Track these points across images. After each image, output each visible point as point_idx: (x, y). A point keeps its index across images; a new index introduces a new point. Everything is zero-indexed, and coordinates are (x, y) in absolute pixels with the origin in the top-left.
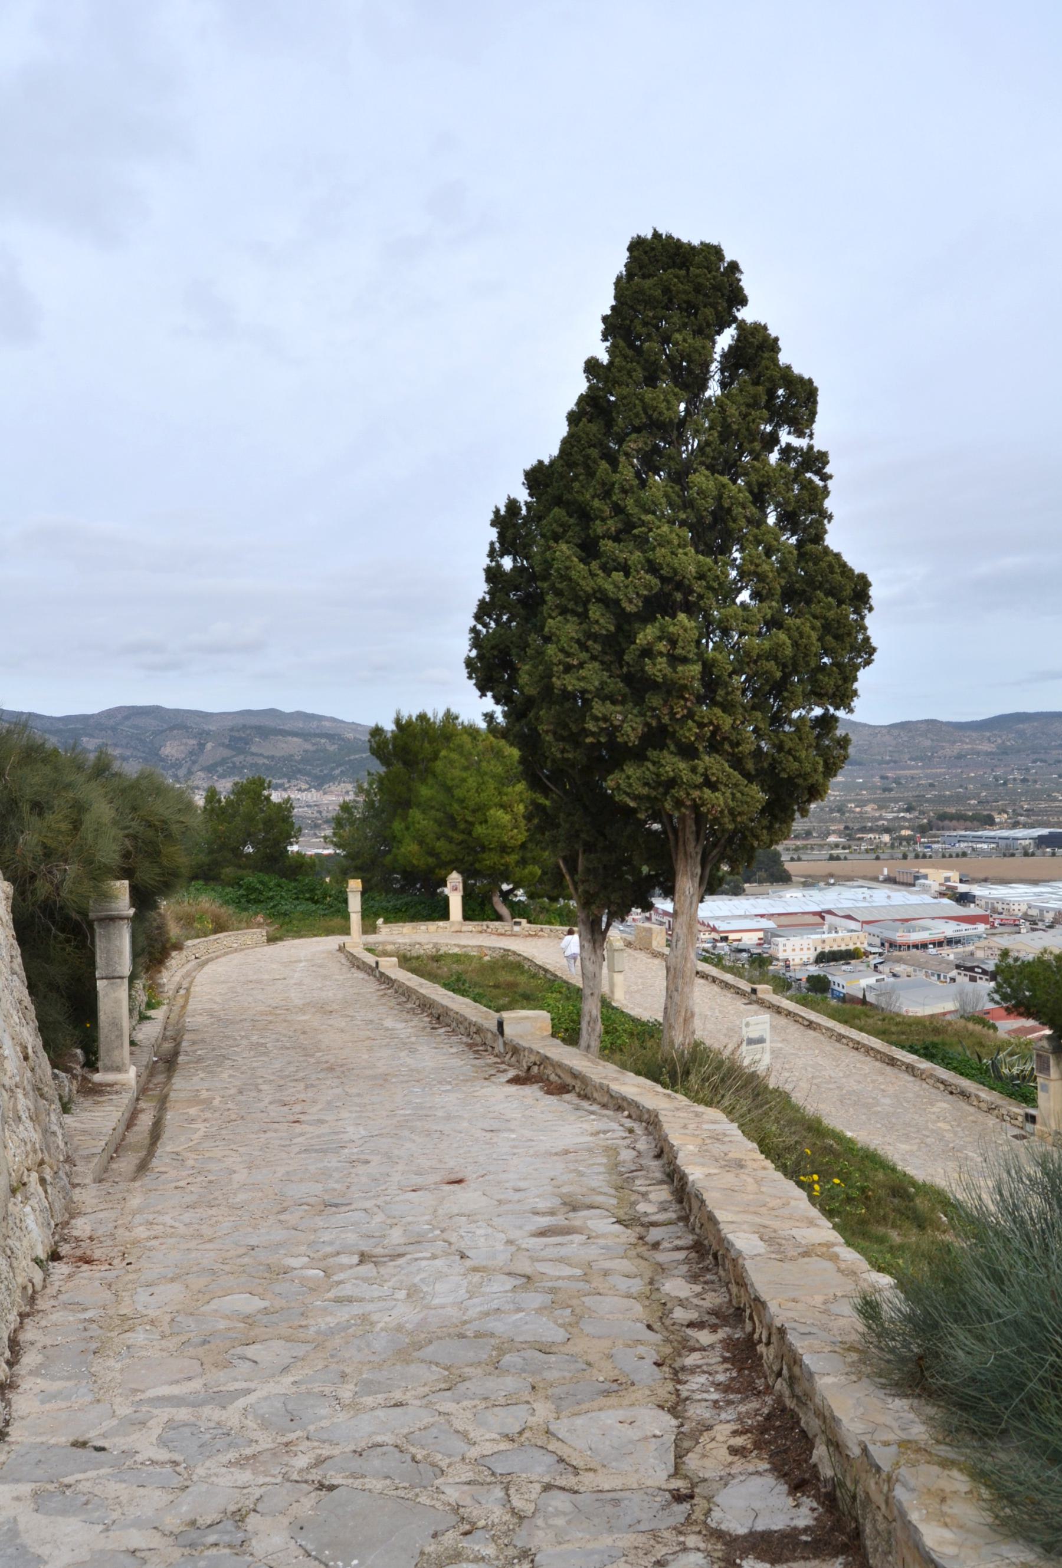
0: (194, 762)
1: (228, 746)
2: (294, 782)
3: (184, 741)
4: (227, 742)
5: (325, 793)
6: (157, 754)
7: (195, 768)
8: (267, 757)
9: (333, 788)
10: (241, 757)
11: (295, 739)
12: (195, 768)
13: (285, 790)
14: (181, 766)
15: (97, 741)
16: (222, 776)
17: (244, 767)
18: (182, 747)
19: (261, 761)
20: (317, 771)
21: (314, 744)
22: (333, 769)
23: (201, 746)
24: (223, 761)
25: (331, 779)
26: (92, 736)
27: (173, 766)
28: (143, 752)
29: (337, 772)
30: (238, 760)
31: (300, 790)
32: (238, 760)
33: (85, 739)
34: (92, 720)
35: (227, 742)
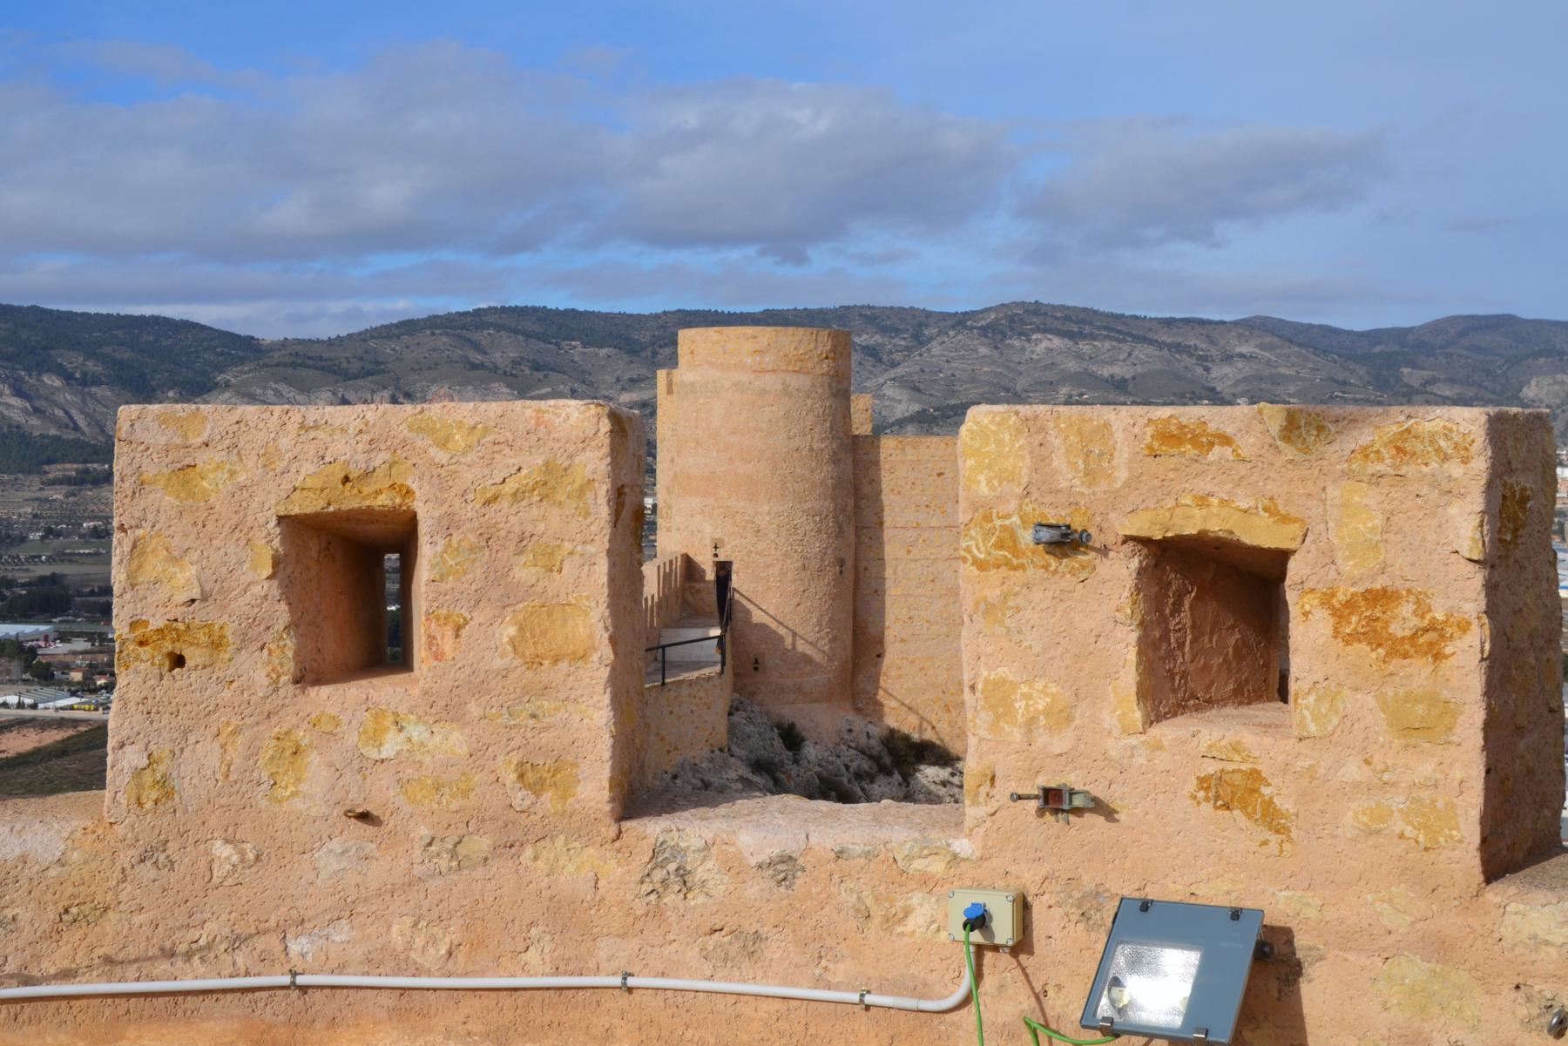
3: (1559, 377)
15: (1424, 373)
18: (1556, 387)
26: (1415, 366)
28: (1494, 392)
33: (1405, 371)
34: (1411, 337)
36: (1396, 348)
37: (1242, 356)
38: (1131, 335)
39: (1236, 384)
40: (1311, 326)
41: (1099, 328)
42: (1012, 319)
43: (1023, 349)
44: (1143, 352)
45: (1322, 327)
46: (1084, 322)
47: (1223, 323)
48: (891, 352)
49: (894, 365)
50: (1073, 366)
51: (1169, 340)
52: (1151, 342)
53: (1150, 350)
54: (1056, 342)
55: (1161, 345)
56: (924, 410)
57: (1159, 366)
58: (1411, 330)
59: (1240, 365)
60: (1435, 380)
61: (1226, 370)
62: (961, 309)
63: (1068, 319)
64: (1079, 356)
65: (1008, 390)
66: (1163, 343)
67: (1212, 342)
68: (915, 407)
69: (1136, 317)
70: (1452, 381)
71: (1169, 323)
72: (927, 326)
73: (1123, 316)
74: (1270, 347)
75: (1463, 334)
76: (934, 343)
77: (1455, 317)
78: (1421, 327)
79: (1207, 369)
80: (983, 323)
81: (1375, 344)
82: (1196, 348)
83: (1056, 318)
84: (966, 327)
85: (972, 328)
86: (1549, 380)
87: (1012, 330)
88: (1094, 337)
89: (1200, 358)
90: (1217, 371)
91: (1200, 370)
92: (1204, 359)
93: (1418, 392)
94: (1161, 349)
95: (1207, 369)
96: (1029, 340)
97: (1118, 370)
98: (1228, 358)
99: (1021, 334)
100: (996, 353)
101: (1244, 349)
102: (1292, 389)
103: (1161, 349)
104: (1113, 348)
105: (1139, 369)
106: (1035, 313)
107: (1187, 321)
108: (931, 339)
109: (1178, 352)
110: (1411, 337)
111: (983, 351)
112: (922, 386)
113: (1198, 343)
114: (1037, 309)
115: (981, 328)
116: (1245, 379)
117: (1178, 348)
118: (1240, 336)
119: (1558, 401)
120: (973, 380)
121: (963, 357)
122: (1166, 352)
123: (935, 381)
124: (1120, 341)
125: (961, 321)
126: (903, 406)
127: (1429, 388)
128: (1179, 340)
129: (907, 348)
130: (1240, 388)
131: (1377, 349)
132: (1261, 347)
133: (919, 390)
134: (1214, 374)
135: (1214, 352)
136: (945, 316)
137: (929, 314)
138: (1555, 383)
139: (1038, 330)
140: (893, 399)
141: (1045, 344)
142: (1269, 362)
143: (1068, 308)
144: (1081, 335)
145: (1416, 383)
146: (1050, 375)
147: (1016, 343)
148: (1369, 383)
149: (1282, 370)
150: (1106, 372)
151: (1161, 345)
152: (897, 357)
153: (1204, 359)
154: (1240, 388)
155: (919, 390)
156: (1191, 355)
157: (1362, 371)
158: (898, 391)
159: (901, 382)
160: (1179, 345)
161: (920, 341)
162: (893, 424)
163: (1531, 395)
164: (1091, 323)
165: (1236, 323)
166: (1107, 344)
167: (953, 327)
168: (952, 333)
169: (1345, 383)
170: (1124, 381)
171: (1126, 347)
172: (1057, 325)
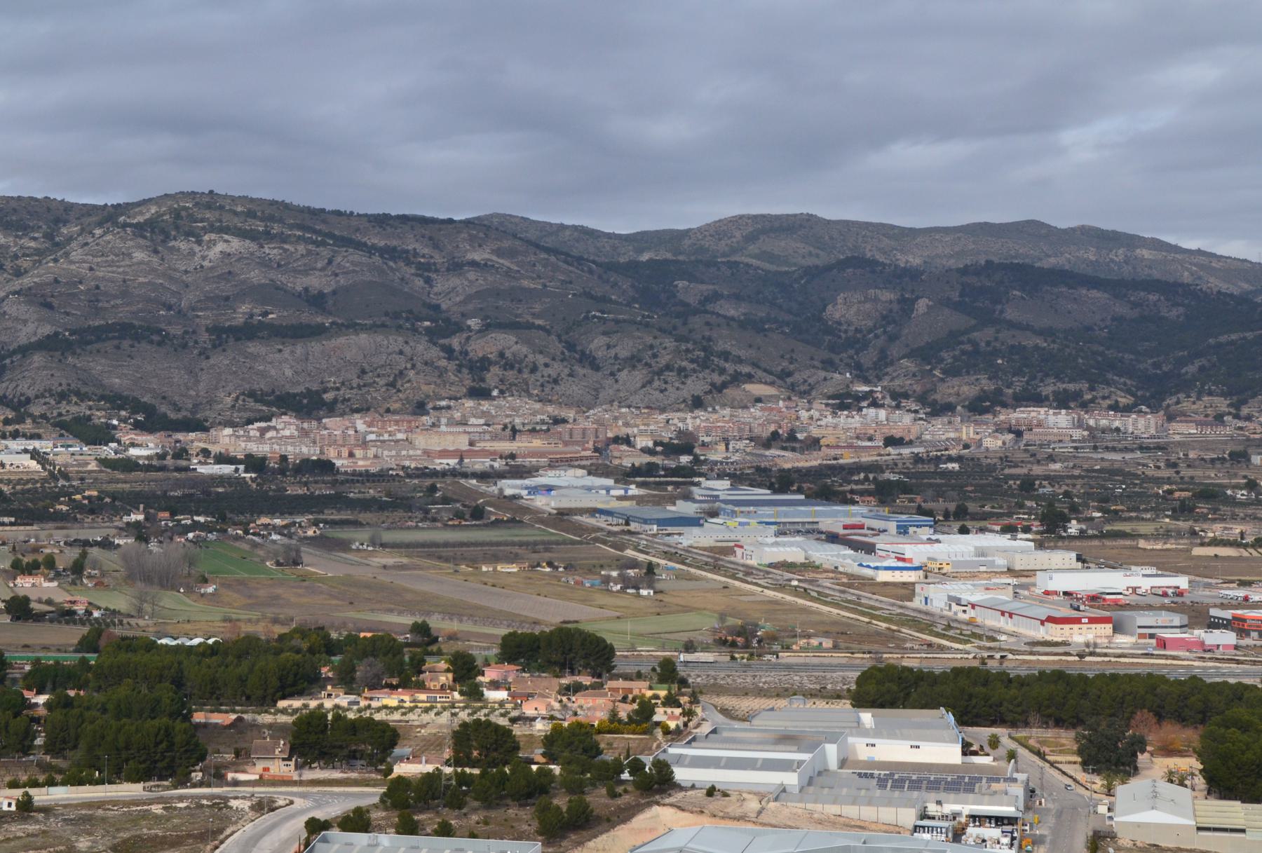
0: (893, 338)
1: (958, 307)
2: (1103, 390)
4: (955, 296)
5: (1171, 418)
6: (820, 319)
7: (895, 350)
8: (1041, 333)
9: (1186, 405)
10: (989, 332)
11: (1094, 293)
12: (895, 350)
13: (1084, 406)
14: (865, 346)
15: (703, 287)
16: (952, 372)
17: (996, 353)
19: (1031, 341)
20: (1147, 365)
21: (1135, 305)
22: (1182, 362)
23: (907, 305)
24: (953, 338)
25: (1185, 386)
26: (692, 278)
27: (850, 343)
29: (1191, 369)
30: (983, 336)
31: (1115, 407)
32: (983, 336)
33: (681, 284)
34: (687, 242)
35: (955, 296)
36: (669, 256)
37: (474, 264)
38: (332, 236)
39: (464, 302)
40: (562, 227)
41: (291, 227)
42: (177, 214)
43: (192, 254)
44: (349, 259)
45: (575, 228)
46: (271, 218)
47: (450, 221)
48: (16, 257)
49: (19, 273)
50: (255, 276)
51: (382, 244)
52: (360, 246)
53: (357, 256)
54: (236, 244)
55: (371, 250)
56: (56, 334)
57: (368, 277)
58: (686, 233)
59: (472, 275)
60: (716, 296)
61: (455, 281)
62: (112, 201)
63: (250, 214)
64: (265, 263)
65: (170, 308)
66: (374, 247)
67: (436, 246)
68: (47, 330)
69: (338, 213)
70: (737, 298)
71: (382, 221)
72: (65, 222)
73: (323, 210)
74: (511, 254)
75: (751, 238)
76: (74, 244)
77: (741, 217)
78: (699, 229)
79: (428, 281)
80: (140, 219)
81: (640, 251)
82: (416, 254)
83: (236, 213)
84: (116, 224)
85: (125, 225)
86: (858, 296)
87: (177, 228)
88: (283, 239)
89: (420, 266)
90: (442, 284)
91: (419, 282)
92: (425, 270)
93: (696, 312)
94: (371, 255)
95: (428, 281)
96: (199, 242)
97: (315, 282)
98: (456, 267)
99: (188, 234)
100: (155, 260)
101: (477, 256)
102: (538, 308)
103: (371, 255)
104: (309, 252)
105: (342, 281)
106: (209, 207)
107: (404, 219)
108: (70, 239)
109: (393, 259)
110: (687, 242)
111: (139, 255)
112: (55, 302)
113: (417, 246)
114: (211, 201)
115: (139, 226)
116: (479, 294)
117: (391, 253)
118: (472, 239)
119: (870, 324)
120: (125, 294)
121: (110, 264)
122: (377, 259)
123: (73, 295)
124: (317, 244)
125: (110, 216)
126: (31, 327)
127: (709, 307)
128: (395, 243)
129: (39, 253)
130: (470, 307)
131: (645, 257)
132: (499, 252)
133: (50, 306)
134: (438, 287)
135: (438, 258)
136: (90, 210)
137: (68, 207)
138: (867, 300)
139: (212, 229)
140: (17, 319)
141: (220, 247)
142: (508, 273)
143: (252, 200)
144: (268, 236)
145: (692, 300)
146: (226, 288)
147: (183, 245)
148: (634, 300)
149: (525, 283)
150: (299, 284)
151: (371, 250)
152: (25, 263)
153: (425, 270)
154: (470, 307)
155: (50, 306)
156: (408, 263)
157: (626, 285)
158: (24, 308)
159: (27, 295)
160: (394, 249)
161: (56, 246)
162: (14, 352)
163: (837, 316)
164: (281, 221)
165: (468, 222)
166: (301, 248)
167: (100, 224)
168: (98, 232)
169: (604, 299)
170: (321, 295)
171: (325, 252)
172: (237, 222)
